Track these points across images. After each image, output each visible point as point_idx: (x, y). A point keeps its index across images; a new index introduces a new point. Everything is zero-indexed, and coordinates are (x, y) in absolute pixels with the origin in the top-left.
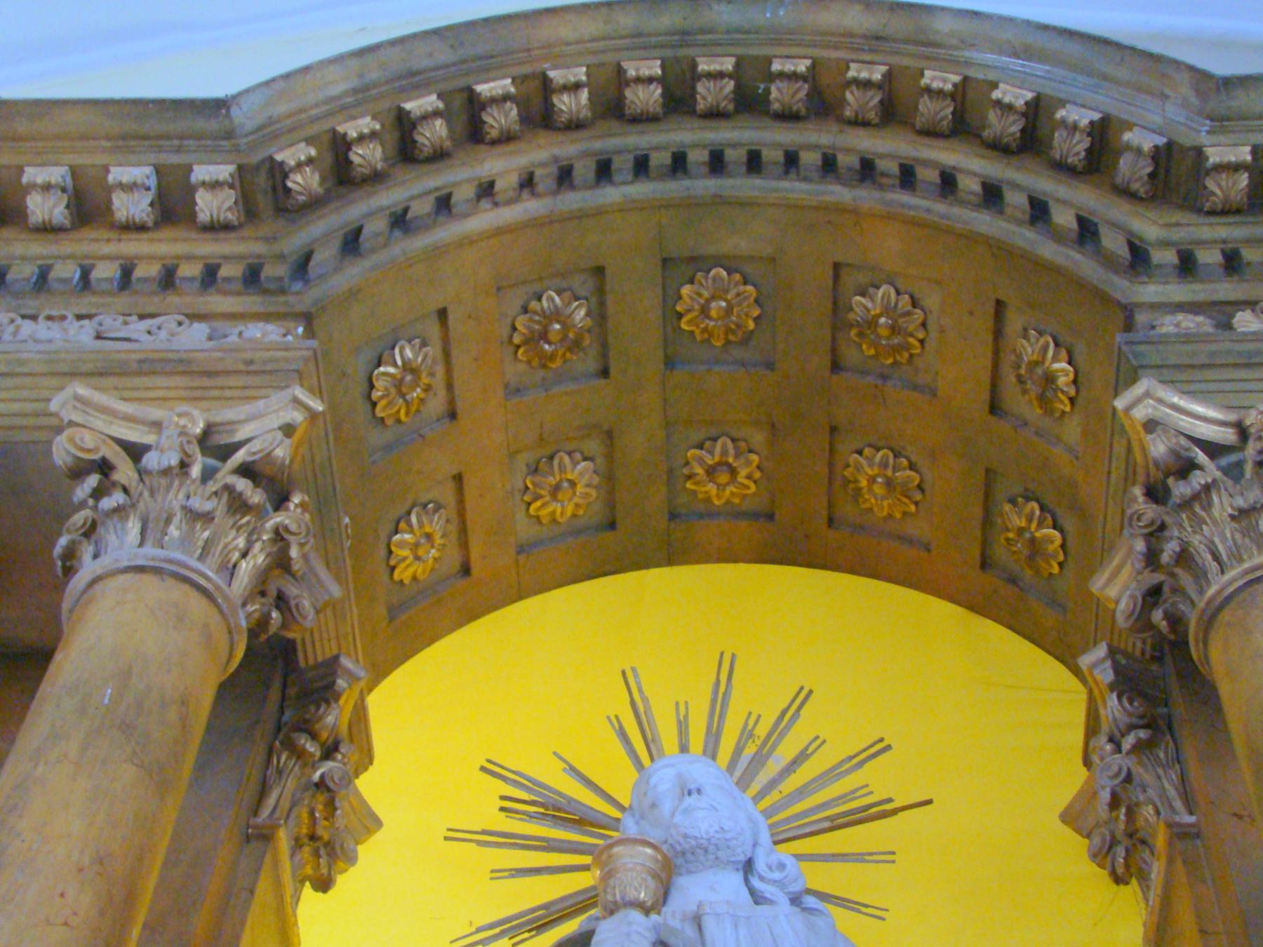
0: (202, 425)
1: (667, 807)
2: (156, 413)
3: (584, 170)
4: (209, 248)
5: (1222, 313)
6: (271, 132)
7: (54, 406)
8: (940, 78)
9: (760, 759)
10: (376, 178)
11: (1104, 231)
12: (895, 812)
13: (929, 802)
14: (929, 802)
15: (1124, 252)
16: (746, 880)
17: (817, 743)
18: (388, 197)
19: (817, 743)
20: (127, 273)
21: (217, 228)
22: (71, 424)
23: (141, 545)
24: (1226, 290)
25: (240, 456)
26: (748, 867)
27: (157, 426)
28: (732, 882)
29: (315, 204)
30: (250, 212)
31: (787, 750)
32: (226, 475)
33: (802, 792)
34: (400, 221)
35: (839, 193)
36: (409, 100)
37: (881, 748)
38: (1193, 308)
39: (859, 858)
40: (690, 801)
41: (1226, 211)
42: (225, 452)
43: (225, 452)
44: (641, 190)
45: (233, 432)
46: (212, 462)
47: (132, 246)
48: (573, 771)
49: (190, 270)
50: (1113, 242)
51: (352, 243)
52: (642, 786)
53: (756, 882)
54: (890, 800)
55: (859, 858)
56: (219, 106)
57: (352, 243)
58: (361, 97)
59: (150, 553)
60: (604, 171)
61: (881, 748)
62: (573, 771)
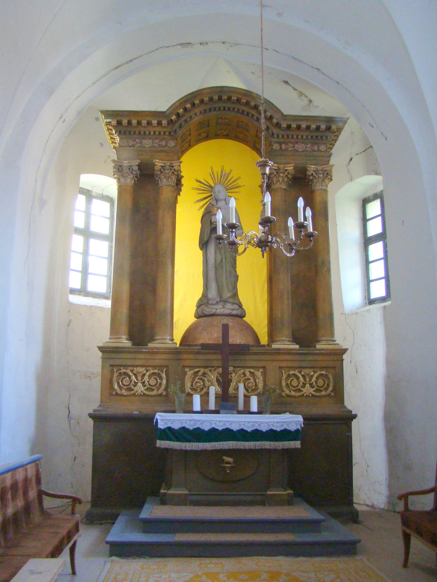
0: (170, 163)
1: (217, 193)
2: (164, 162)
3: (208, 111)
4: (164, 130)
5: (280, 144)
6: (171, 114)
7: (154, 161)
8: (253, 104)
9: (226, 179)
10: (183, 115)
11: (270, 129)
12: (240, 187)
13: (244, 186)
14: (244, 186)
15: (271, 134)
16: (225, 201)
17: (233, 177)
18: (184, 119)
19: (233, 177)
20: (155, 132)
21: (165, 127)
22: (157, 165)
23: (166, 182)
24: (282, 140)
25: (174, 168)
26: (225, 200)
27: (165, 163)
28: (224, 202)
29: (176, 121)
30: (168, 123)
31: (229, 178)
32: (173, 171)
33: (231, 184)
34: (186, 121)
35: (239, 115)
36: (187, 105)
37: (239, 178)
38: (277, 142)
39: (237, 192)
40: (220, 194)
41: (283, 130)
42: (173, 167)
43: (173, 167)
44: (215, 113)
45: (173, 164)
46: (171, 168)
47: (155, 129)
48: (205, 180)
49: (162, 133)
50: (270, 132)
51: (180, 127)
52: (214, 186)
53: (227, 202)
54: (240, 185)
55: (237, 192)
56: (164, 113)
57: (180, 127)
58: (181, 104)
59: (168, 184)
60: (210, 110)
61: (239, 178)
62: (205, 180)
